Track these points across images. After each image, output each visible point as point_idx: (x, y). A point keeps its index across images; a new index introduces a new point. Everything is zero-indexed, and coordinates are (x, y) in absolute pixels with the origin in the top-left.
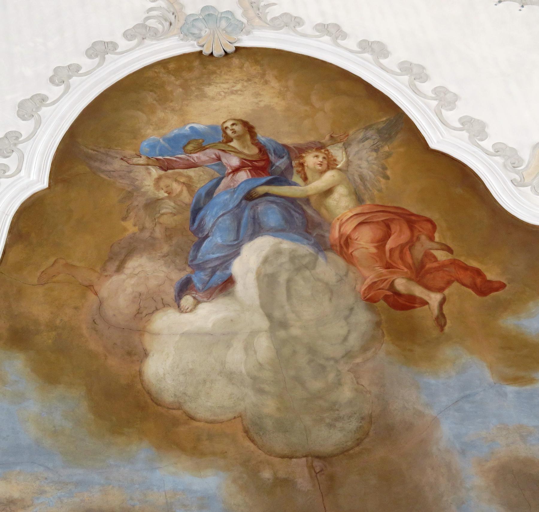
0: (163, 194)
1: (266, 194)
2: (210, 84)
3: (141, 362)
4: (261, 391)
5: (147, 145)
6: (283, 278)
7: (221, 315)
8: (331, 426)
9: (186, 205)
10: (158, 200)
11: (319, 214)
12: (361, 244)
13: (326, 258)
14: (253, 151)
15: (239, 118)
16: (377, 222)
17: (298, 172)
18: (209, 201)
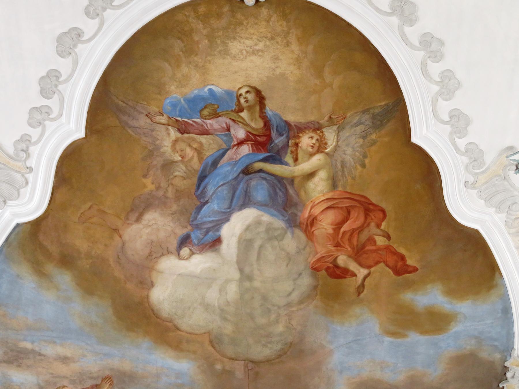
0: (177, 158)
1: (261, 171)
2: (234, 38)
3: (149, 289)
4: (225, 319)
5: (170, 102)
6: (257, 244)
7: (208, 265)
8: (264, 345)
9: (195, 170)
10: (173, 162)
11: (298, 195)
12: (322, 225)
13: (293, 233)
15: (254, 85)
16: (341, 208)
17: (292, 152)
18: (213, 170)
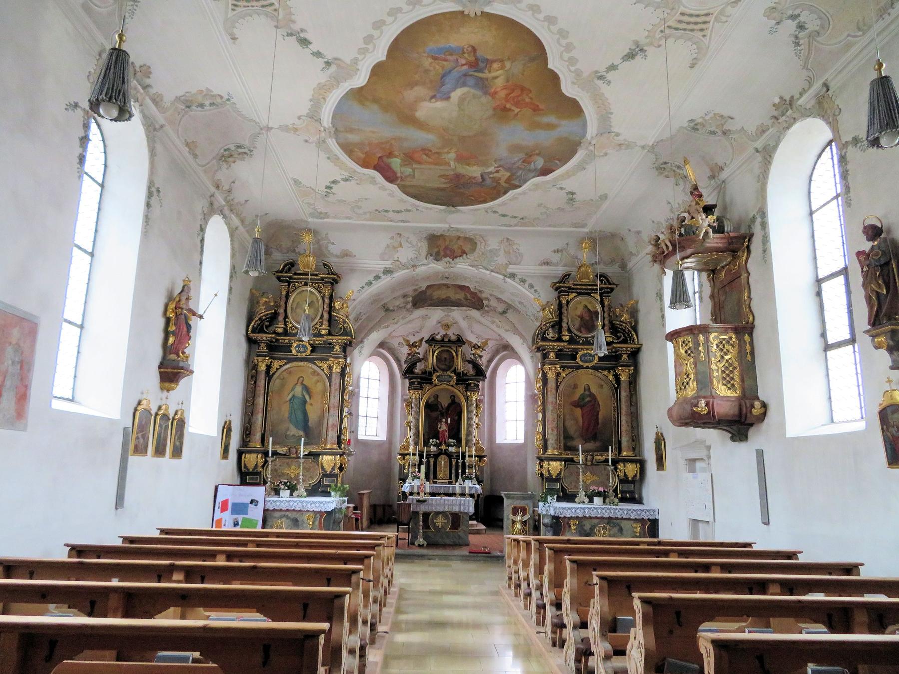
0: (431, 69)
1: (471, 75)
6: (468, 100)
10: (429, 71)
14: (472, 59)
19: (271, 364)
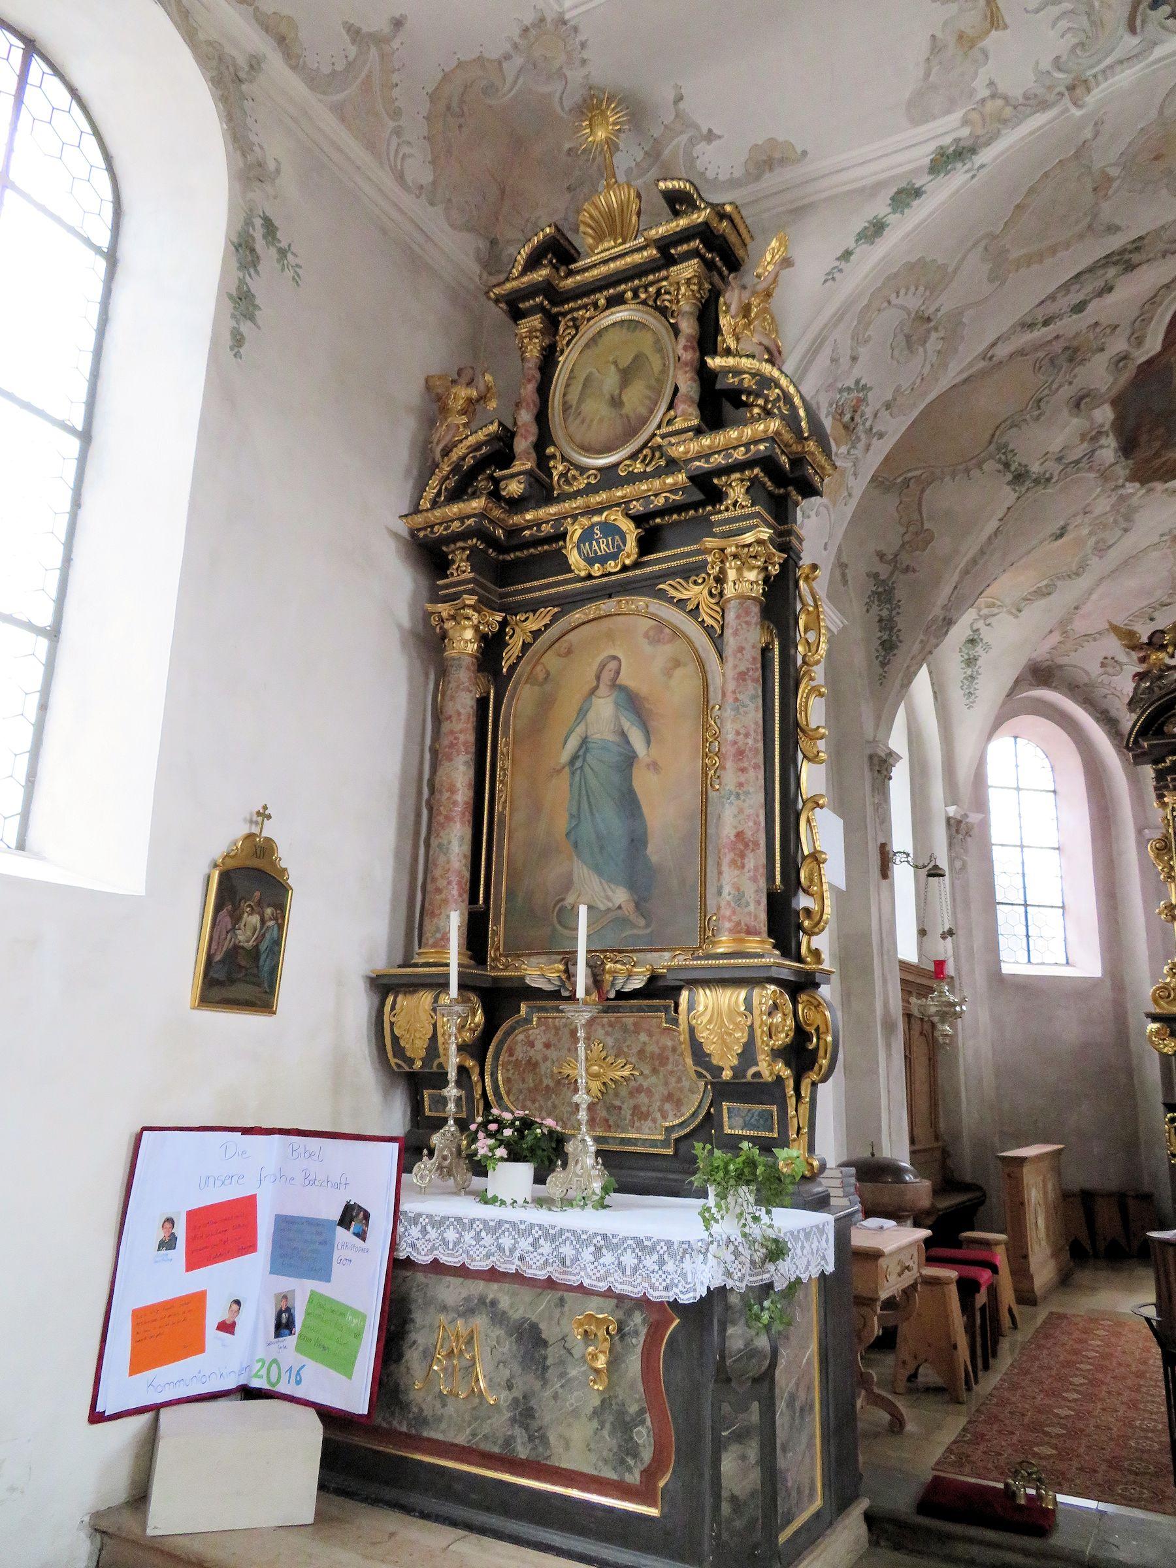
19: (501, 632)
